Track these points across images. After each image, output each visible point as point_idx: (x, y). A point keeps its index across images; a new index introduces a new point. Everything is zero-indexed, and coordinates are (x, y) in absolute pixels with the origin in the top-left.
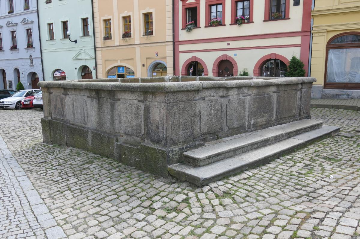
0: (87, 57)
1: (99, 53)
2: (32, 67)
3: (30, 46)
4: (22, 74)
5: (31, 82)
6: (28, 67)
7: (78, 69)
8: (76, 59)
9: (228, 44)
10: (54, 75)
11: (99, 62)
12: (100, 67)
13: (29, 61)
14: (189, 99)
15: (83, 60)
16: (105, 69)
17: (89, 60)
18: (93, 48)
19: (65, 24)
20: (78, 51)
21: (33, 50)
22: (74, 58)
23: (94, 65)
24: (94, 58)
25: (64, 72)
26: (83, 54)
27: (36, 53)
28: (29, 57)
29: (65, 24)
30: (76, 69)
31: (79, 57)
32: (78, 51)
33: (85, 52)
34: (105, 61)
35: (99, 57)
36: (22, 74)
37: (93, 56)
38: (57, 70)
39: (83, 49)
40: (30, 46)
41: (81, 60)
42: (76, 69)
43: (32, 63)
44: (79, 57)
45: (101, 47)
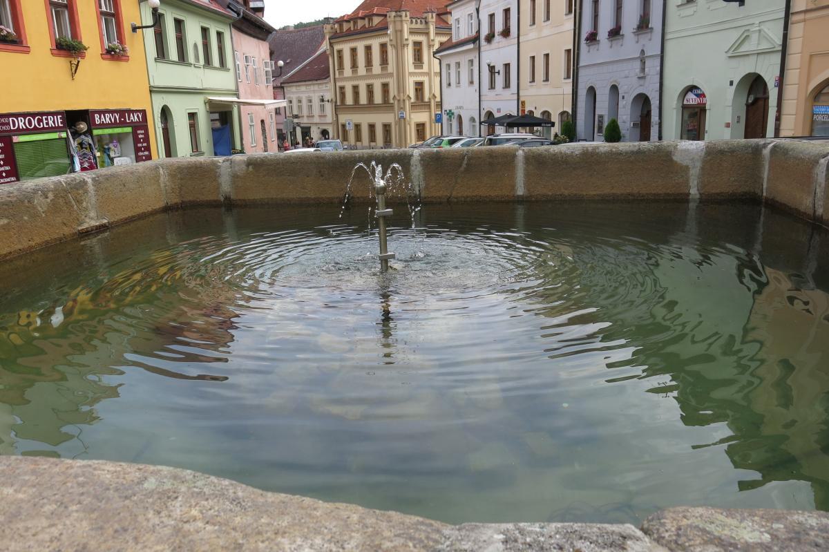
0: (765, 46)
1: (796, 31)
2: (642, 82)
3: (643, 25)
4: (623, 97)
5: (640, 119)
6: (634, 80)
7: (735, 84)
8: (735, 55)
9: (518, 296)
10: (685, 102)
11: (794, 61)
12: (792, 76)
13: (638, 64)
14: (362, 527)
15: (751, 57)
16: (808, 83)
17: (767, 56)
18: (783, 15)
19: (547, 56)
20: (743, 29)
21: (649, 35)
22: (731, 52)
23: (777, 73)
24: (780, 48)
25: (703, 95)
26: (754, 37)
27: (653, 48)
28: (638, 55)
29: (547, 56)
30: (731, 83)
31: (745, 48)
32: (743, 29)
33: (760, 31)
34: (811, 56)
35: (795, 46)
36: (623, 97)
37: (778, 41)
38: (692, 88)
39: (758, 22)
40: (644, 27)
41: (746, 58)
42: (731, 83)
43: (643, 69)
44: (745, 48)
45: (806, 12)
